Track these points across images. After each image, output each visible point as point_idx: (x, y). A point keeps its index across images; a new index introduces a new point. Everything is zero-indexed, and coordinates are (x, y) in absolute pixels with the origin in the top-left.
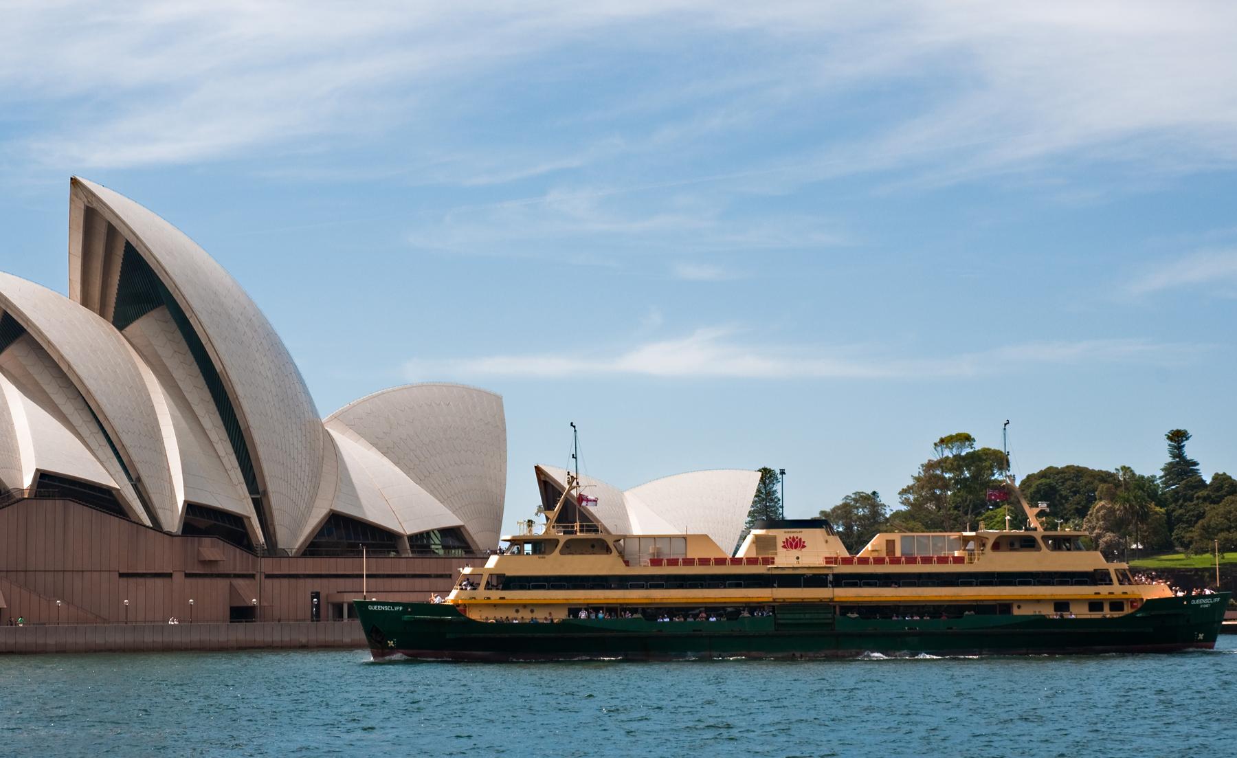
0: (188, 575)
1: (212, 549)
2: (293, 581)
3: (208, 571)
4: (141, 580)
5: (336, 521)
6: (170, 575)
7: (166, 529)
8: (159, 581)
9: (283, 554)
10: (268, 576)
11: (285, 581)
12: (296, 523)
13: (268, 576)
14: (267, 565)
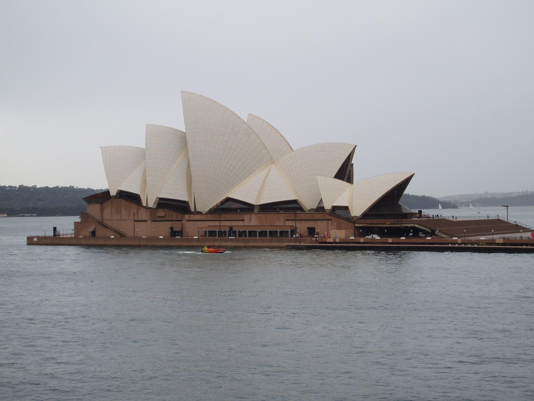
0: (152, 221)
1: (161, 213)
2: (195, 222)
3: (162, 219)
4: (140, 223)
5: (228, 200)
6: (146, 221)
7: (149, 206)
8: (144, 223)
9: (200, 213)
10: (187, 221)
11: (192, 222)
12: (205, 202)
13: (187, 221)
14: (187, 217)
